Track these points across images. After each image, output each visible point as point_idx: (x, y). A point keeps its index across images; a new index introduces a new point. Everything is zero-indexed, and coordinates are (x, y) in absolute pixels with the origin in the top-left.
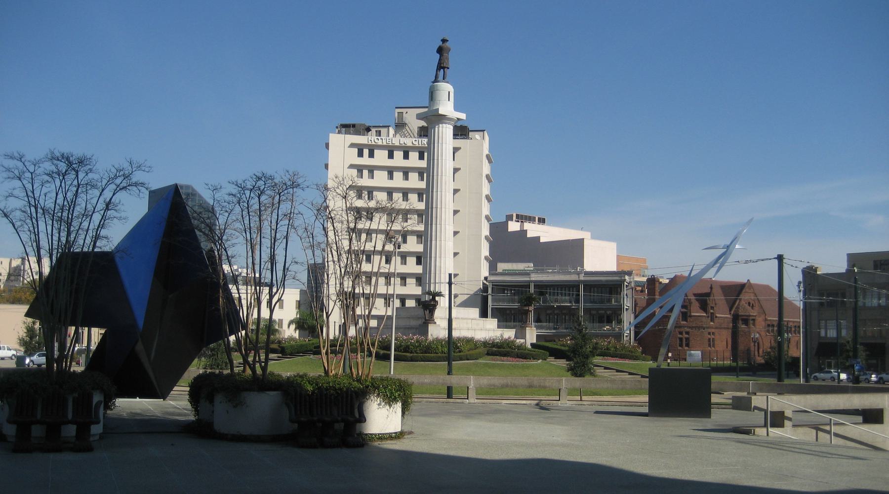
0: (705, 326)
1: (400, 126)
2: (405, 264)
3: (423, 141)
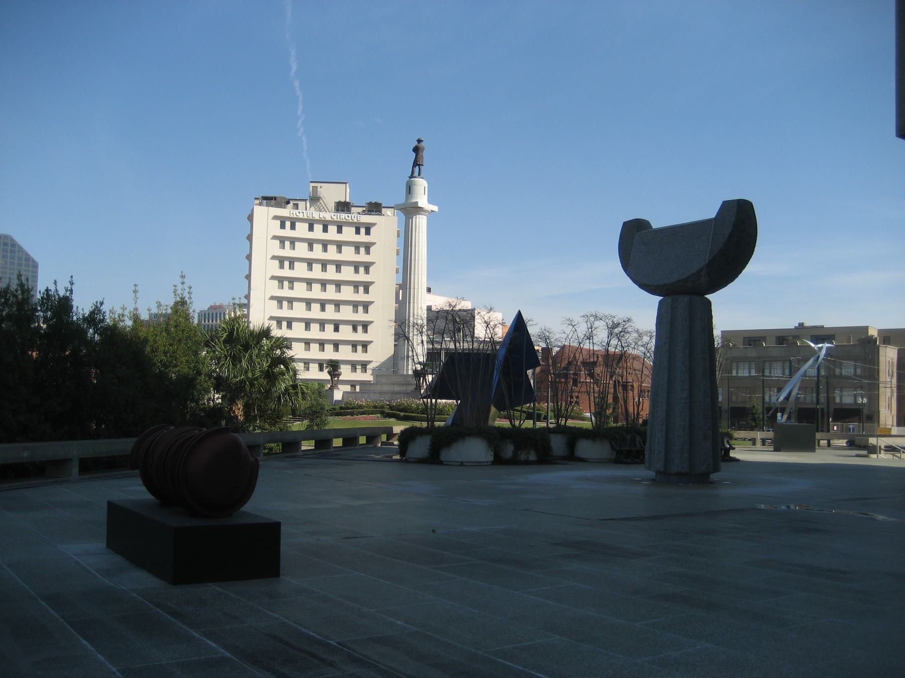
1: (315, 199)
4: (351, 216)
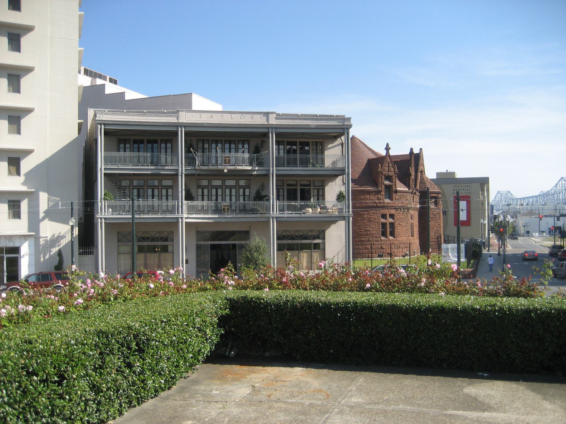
0: (409, 206)
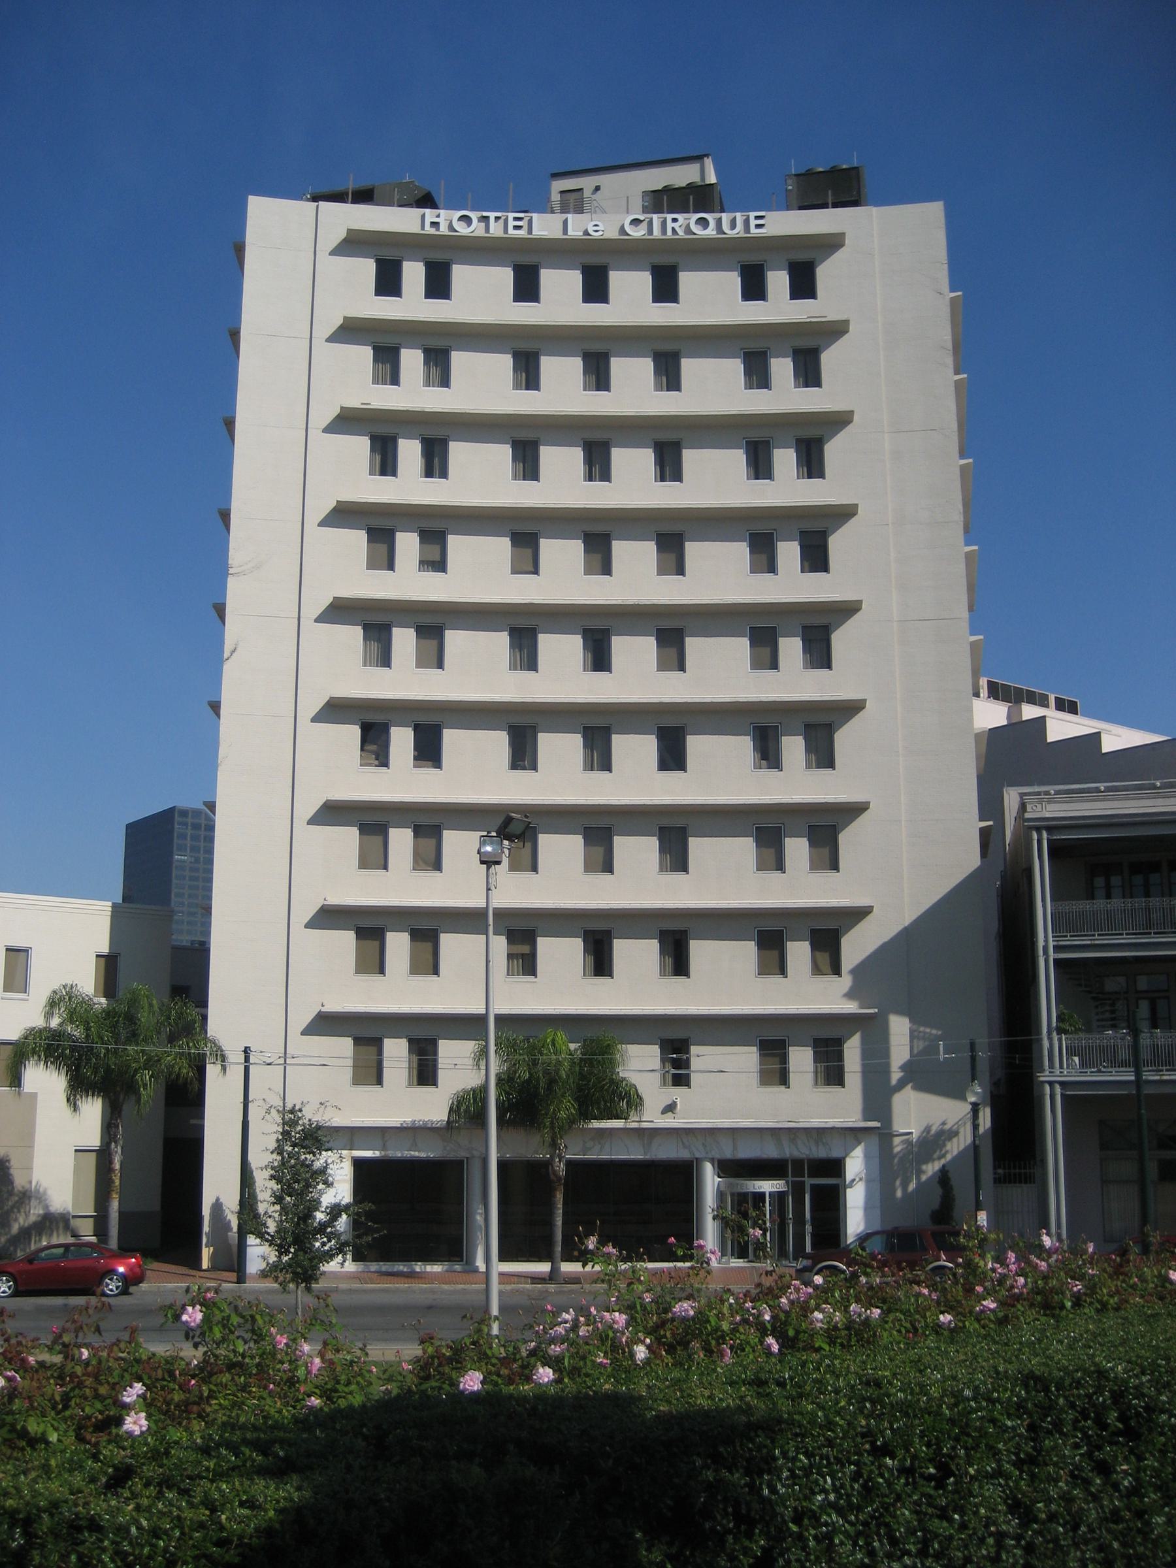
2: (606, 766)
3: (670, 225)
4: (719, 222)
